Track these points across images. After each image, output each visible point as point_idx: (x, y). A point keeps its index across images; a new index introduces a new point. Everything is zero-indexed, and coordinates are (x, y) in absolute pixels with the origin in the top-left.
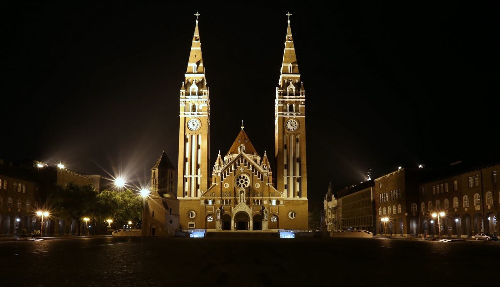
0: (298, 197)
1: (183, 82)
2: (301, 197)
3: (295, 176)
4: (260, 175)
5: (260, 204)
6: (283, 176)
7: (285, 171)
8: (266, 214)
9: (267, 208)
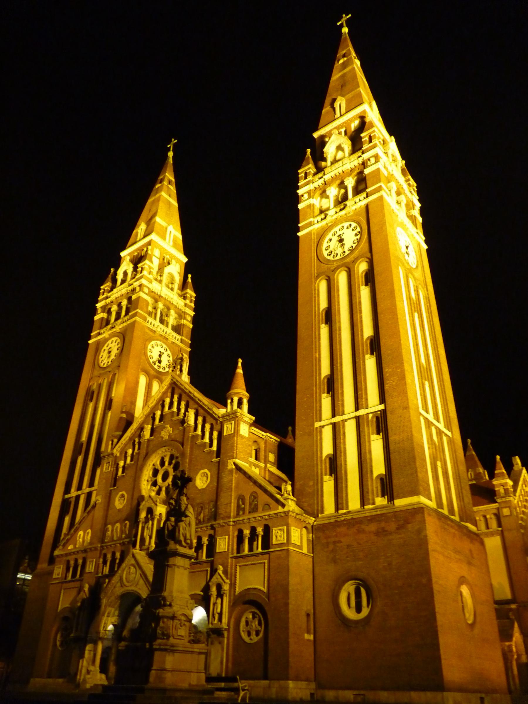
0: (381, 501)
1: (112, 269)
2: (391, 499)
3: (362, 412)
4: (215, 434)
5: (207, 557)
6: (317, 425)
7: (326, 401)
8: (219, 601)
9: (225, 572)
